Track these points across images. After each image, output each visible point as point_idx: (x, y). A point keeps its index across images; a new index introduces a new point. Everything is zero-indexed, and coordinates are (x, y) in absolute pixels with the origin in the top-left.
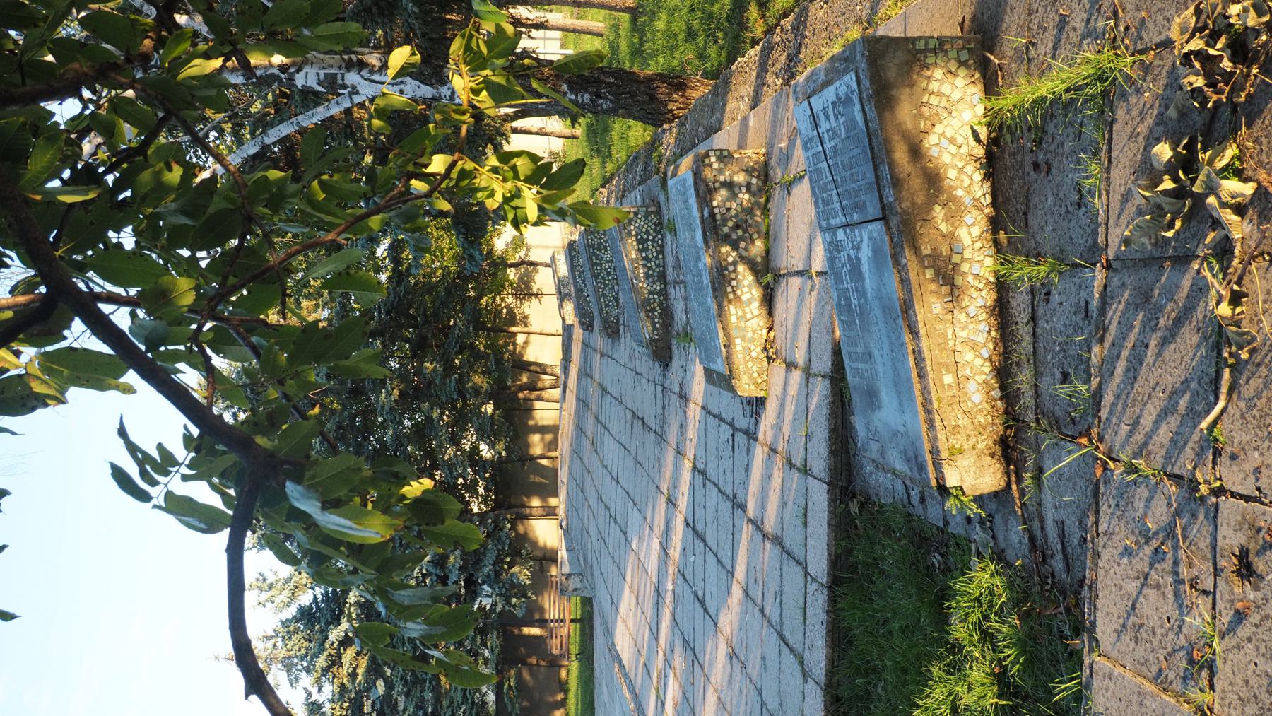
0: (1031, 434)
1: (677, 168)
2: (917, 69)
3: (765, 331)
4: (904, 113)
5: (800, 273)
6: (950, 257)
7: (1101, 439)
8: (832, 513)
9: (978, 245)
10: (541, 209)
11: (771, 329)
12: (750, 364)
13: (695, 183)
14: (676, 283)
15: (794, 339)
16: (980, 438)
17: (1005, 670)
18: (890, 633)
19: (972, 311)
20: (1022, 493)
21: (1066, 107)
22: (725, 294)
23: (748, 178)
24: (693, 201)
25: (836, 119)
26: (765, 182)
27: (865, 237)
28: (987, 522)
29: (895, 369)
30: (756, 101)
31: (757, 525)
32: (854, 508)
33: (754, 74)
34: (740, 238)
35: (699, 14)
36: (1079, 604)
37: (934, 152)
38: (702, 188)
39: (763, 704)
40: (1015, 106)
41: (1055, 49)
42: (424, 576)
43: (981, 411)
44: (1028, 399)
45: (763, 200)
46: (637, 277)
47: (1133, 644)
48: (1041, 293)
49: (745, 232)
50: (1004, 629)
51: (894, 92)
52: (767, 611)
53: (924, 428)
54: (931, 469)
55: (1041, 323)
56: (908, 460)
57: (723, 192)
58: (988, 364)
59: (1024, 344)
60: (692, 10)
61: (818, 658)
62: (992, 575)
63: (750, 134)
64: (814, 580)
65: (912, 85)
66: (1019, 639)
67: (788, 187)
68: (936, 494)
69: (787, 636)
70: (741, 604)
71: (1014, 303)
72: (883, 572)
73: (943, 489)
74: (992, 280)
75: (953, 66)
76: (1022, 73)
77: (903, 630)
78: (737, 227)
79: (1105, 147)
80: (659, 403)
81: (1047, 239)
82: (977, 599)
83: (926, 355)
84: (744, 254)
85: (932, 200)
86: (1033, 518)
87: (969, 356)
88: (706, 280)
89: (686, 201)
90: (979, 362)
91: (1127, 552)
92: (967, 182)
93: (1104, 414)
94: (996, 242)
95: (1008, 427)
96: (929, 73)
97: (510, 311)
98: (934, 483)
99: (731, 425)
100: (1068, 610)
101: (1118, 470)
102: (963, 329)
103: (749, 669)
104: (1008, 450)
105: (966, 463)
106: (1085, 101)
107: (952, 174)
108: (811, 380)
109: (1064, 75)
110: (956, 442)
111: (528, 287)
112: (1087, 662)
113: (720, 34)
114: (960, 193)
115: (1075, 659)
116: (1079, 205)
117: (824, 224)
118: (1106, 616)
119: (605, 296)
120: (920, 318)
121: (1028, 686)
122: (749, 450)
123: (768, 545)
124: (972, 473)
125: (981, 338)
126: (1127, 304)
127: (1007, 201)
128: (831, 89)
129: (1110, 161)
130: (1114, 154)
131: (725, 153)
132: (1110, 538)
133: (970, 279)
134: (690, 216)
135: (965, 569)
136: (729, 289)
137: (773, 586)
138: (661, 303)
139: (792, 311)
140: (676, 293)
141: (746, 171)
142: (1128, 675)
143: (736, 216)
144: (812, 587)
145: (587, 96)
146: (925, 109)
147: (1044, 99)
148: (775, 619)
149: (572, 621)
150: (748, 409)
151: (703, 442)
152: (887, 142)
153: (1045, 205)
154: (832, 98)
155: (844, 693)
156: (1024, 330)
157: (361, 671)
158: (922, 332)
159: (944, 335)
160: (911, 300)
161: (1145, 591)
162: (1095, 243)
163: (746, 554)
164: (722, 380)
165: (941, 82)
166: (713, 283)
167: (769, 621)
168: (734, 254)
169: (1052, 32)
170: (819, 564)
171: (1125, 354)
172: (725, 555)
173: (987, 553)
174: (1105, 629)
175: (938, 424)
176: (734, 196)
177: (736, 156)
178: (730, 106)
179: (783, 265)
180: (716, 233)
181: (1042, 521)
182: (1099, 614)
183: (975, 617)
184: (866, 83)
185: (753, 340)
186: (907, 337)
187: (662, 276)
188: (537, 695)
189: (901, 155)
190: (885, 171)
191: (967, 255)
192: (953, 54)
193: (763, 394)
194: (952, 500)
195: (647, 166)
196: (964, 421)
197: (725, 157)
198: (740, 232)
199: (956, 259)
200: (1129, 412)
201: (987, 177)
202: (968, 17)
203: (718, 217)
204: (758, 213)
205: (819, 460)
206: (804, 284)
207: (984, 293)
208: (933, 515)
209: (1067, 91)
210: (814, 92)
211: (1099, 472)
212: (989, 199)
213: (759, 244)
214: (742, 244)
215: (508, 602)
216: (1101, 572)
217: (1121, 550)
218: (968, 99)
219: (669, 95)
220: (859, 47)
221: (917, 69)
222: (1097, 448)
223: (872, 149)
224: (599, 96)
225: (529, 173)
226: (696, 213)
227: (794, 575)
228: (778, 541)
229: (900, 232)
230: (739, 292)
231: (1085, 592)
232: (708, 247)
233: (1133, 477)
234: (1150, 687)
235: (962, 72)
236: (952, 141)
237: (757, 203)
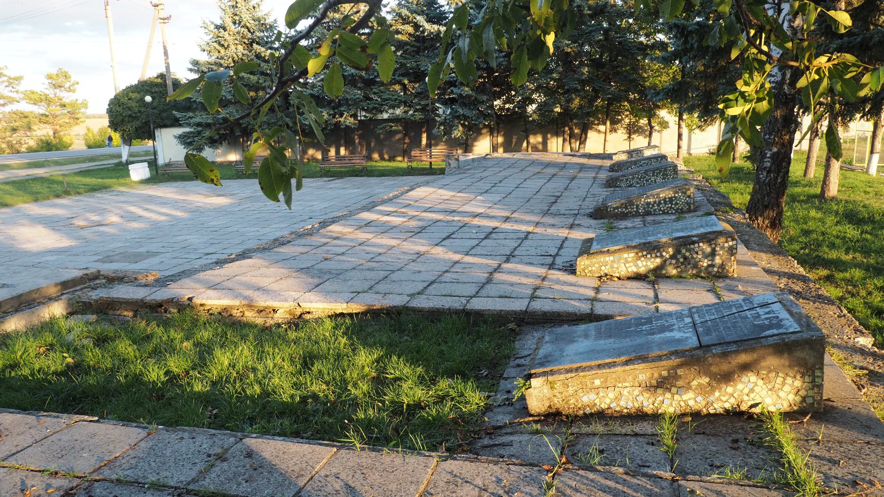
0: (564, 430)
1: (723, 220)
2: (802, 370)
3: (618, 275)
4: (772, 361)
5: (656, 297)
6: (675, 386)
7: (566, 470)
8: (508, 313)
9: (683, 404)
10: (734, 118)
11: (619, 278)
12: (597, 265)
13: (715, 232)
14: (644, 222)
15: (614, 292)
16: (560, 400)
17: (423, 409)
18: (439, 344)
19: (640, 398)
20: (528, 423)
21: (778, 461)
22: (642, 251)
23: (717, 265)
24: (702, 230)
25: (767, 319)
26: (714, 276)
27: (688, 335)
28: (509, 402)
29: (603, 351)
30: (768, 271)
31: (498, 269)
32: (511, 326)
33: (786, 271)
34: (678, 260)
35: (821, 238)
36: (463, 451)
37: (745, 379)
38: (712, 236)
39: (393, 271)
40: (776, 430)
41: (816, 456)
43: (577, 401)
44: (585, 429)
45: (703, 275)
46: (648, 197)
47: (445, 480)
48: (654, 440)
49: (682, 263)
50: (447, 409)
51: (786, 355)
52: (447, 274)
53: (567, 367)
54: (541, 370)
55: (633, 439)
56: (546, 357)
57: (709, 250)
58: (606, 406)
59: (620, 428)
60: (823, 234)
61: (422, 303)
62: (477, 404)
63: (746, 267)
64: (468, 301)
65: (790, 366)
66: (441, 417)
67: (712, 290)
68: (526, 373)
69: (434, 286)
70: (450, 260)
71: (645, 424)
72: (474, 341)
73: (529, 377)
74: (660, 411)
75: (803, 393)
76: (799, 435)
77: (442, 352)
78: (685, 258)
79: (751, 483)
80: (567, 212)
81: (689, 445)
82: (462, 395)
83: (613, 370)
84: (668, 263)
85: (713, 376)
86: (513, 428)
87: (611, 395)
88: (651, 239)
89: (702, 226)
90: (608, 401)
91: (499, 481)
92: (724, 399)
93: (581, 472)
94: (684, 415)
95: (567, 417)
96: (798, 377)
97: (619, 121)
98: (533, 371)
99: (557, 255)
100: (460, 445)
101: (548, 478)
102: (629, 393)
103: (412, 264)
104: (553, 417)
105: (545, 391)
106: (782, 473)
107: (730, 390)
108: (589, 302)
109: (799, 461)
110: (558, 385)
111: (634, 133)
112: (433, 454)
113: (807, 251)
114: (717, 394)
115: (433, 448)
116: (711, 466)
117: (694, 310)
118: (459, 466)
119: (633, 178)
120: (636, 366)
121: (415, 421)
122: (543, 265)
123: (486, 275)
124: (539, 395)
125: (623, 403)
126: (651, 490)
127: (711, 422)
128: (788, 316)
129: (742, 485)
130: (747, 488)
131: (734, 251)
132: (506, 471)
133: (661, 398)
134: (693, 229)
135: (481, 388)
136: (645, 253)
137: (462, 278)
138: (631, 212)
139: (632, 291)
140: (638, 221)
141: (722, 264)
142: (428, 476)
143: (692, 258)
144: (464, 300)
145: (769, 164)
146: (774, 374)
147: (782, 448)
148: (443, 279)
150: (568, 264)
151: (544, 238)
152: (753, 350)
153: (711, 446)
154: (781, 316)
155: (403, 317)
156: (628, 429)
157: (400, 37)
158: (627, 368)
159: (625, 381)
160: (648, 362)
161: (477, 489)
162: (688, 474)
163: (479, 264)
164: (586, 248)
165: (792, 385)
166: (649, 243)
167: (441, 276)
168: (668, 256)
169: (827, 455)
170: (477, 304)
171: (620, 487)
172: (478, 250)
173: (490, 402)
174: (453, 465)
175: (569, 375)
176: (706, 256)
177: (733, 258)
178: (763, 256)
179: (661, 287)
180: (681, 245)
181: (511, 434)
182: (461, 462)
183: (452, 393)
184: (793, 337)
185: (612, 267)
186: (623, 358)
187: (648, 213)
188: (387, 143)
189: (744, 358)
190: (734, 348)
191: (676, 397)
192: (811, 393)
193: (578, 273)
194: (522, 381)
195: (720, 204)
196: (571, 390)
197: (732, 251)
198: (682, 260)
199: (674, 390)
200: (583, 487)
201: (727, 411)
202: (835, 404)
203: (692, 246)
204: (694, 272)
205: (538, 306)
206: (650, 299)
207: (651, 406)
208: (510, 372)
209: (789, 462)
210: (784, 305)
211: (545, 467)
212: (712, 412)
213: (674, 272)
214: (674, 261)
215: (441, 124)
216: (486, 465)
217: (500, 477)
218: (779, 401)
219: (768, 218)
220: (818, 333)
221: (802, 370)
222: (560, 467)
223: (748, 340)
224: (768, 172)
225: (757, 110)
226: (695, 232)
227: (471, 290)
228: (489, 281)
229: (692, 356)
230: (643, 259)
231: (471, 456)
232: (672, 240)
233: (545, 486)
234: (422, 488)
235: (798, 399)
236: (752, 390)
237: (701, 271)
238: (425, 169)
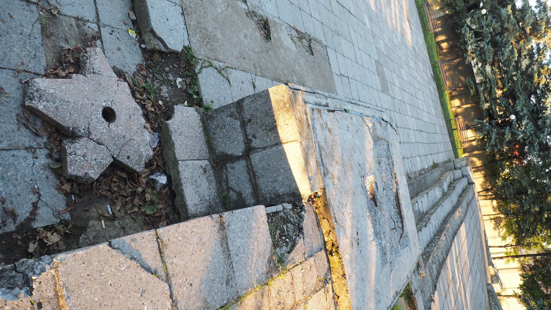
42: (519, 127)
111: (496, 222)
157: (536, 76)
188: (457, 72)
215: (482, 124)
238: (451, 127)
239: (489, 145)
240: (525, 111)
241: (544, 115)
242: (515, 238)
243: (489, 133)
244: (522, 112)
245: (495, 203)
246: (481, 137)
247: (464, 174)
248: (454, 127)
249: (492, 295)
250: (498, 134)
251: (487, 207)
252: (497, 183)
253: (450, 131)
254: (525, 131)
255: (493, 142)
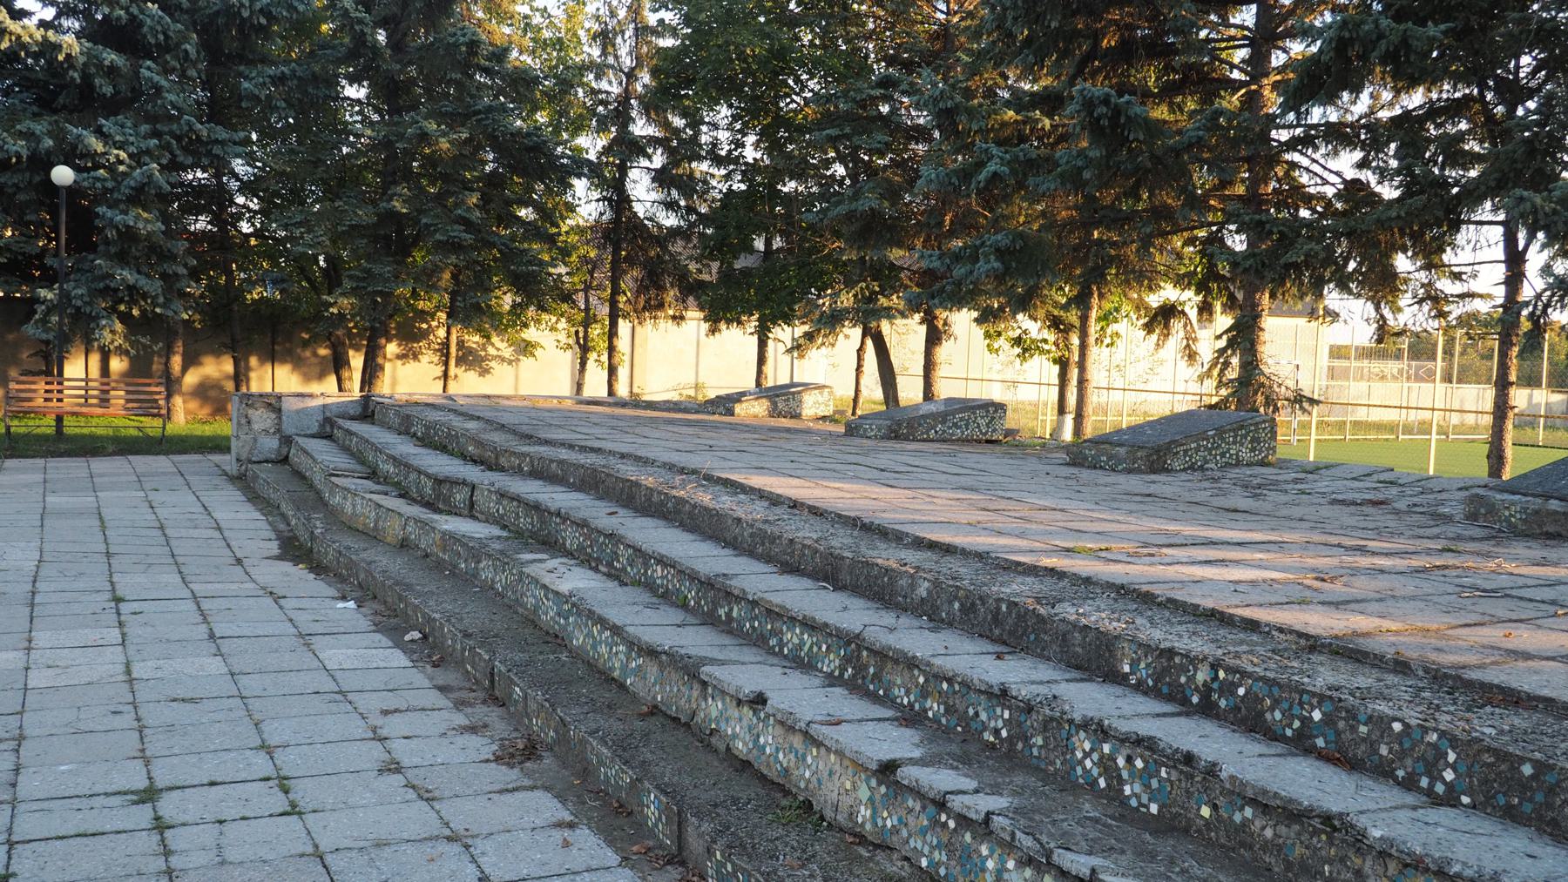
97: (424, 335)
119: (1197, 450)
149: (59, 419)
239: (163, 306)
240: (39, 128)
241: (82, 59)
242: (542, 308)
243: (107, 292)
244: (39, 140)
245: (392, 348)
246: (119, 327)
247: (315, 429)
248: (46, 426)
249: (910, 426)
250: (122, 258)
251: (410, 378)
252: (341, 316)
253: (63, 446)
254: (132, 149)
255: (153, 286)
